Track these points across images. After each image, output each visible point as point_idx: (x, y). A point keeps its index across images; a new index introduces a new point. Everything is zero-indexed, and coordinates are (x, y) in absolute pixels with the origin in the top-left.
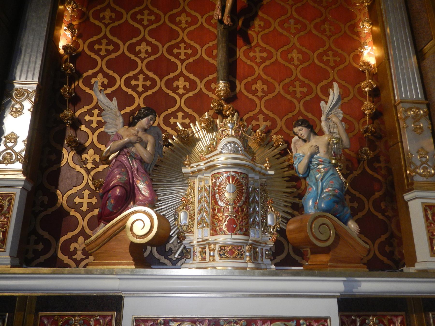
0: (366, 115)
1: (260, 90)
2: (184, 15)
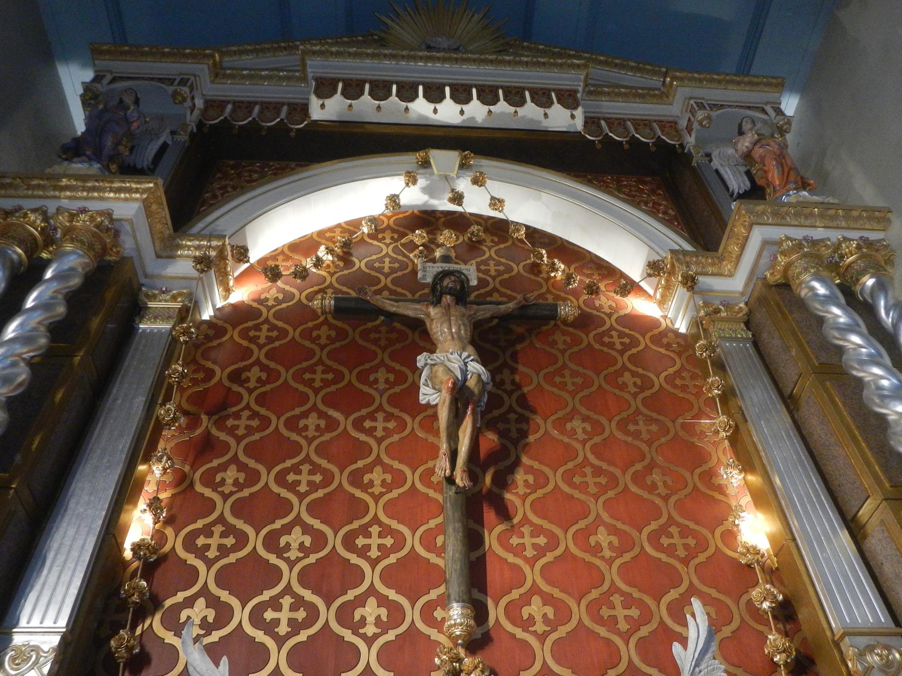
0: (776, 665)
1: (538, 618)
2: (378, 469)
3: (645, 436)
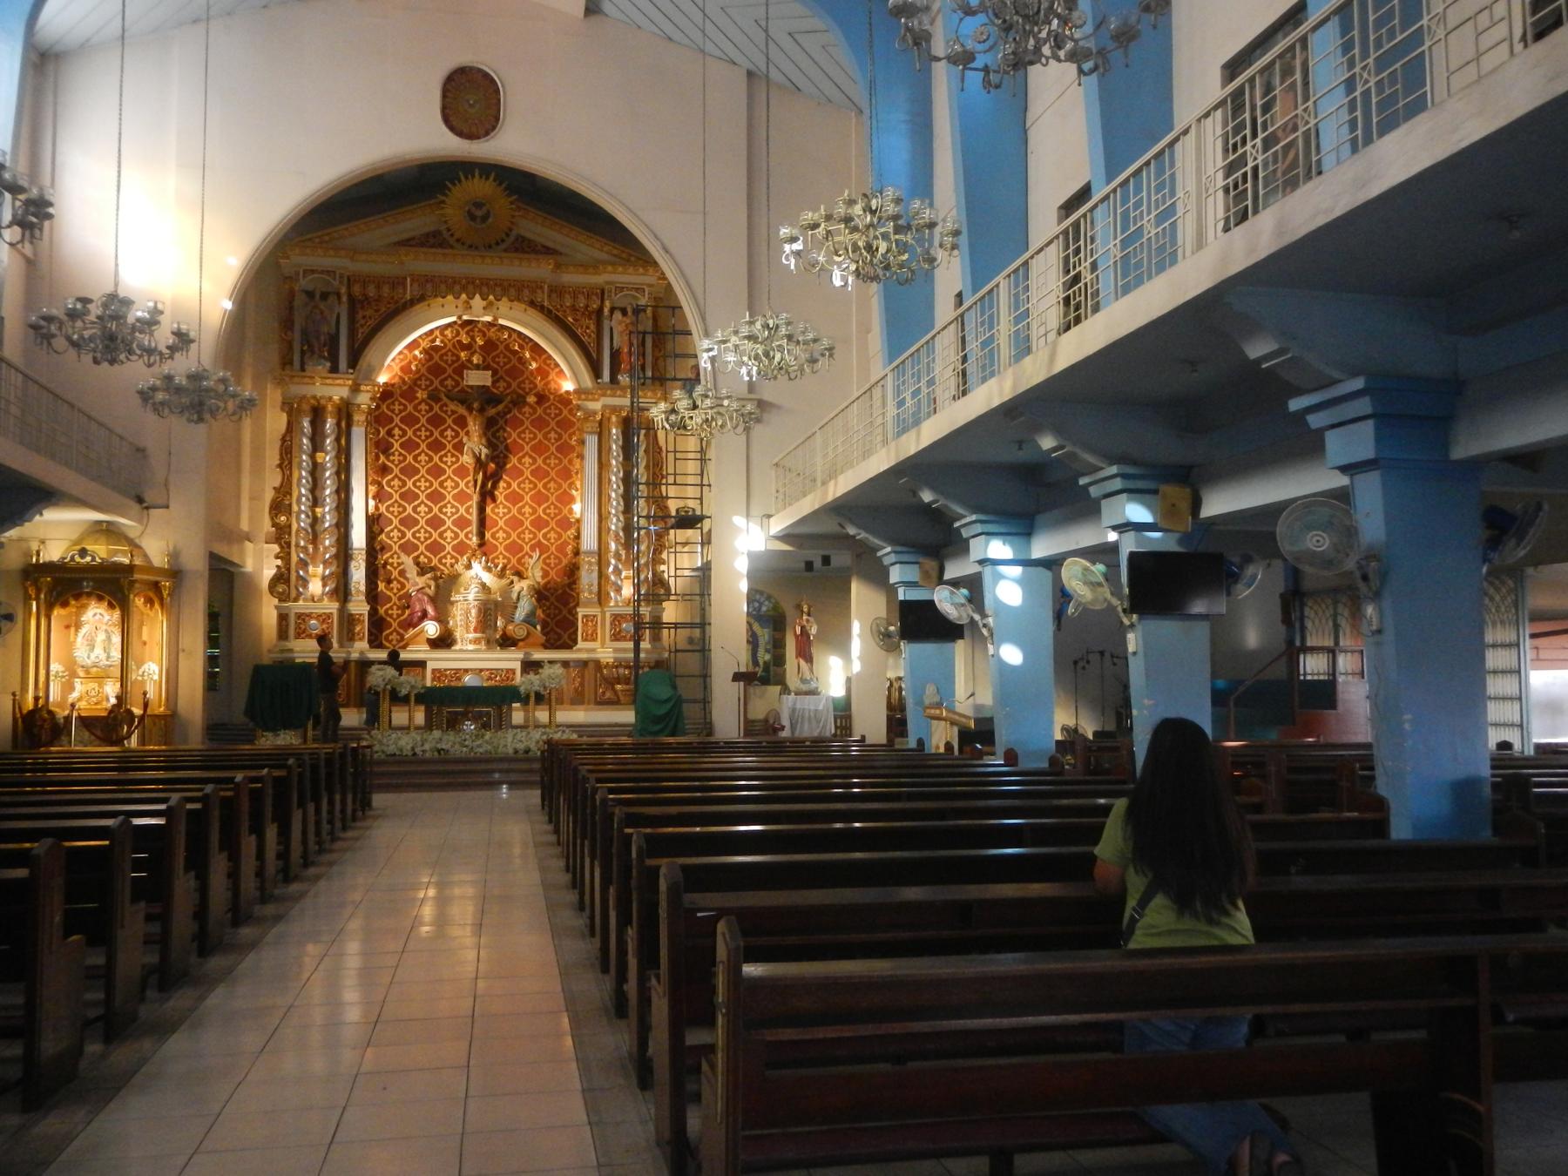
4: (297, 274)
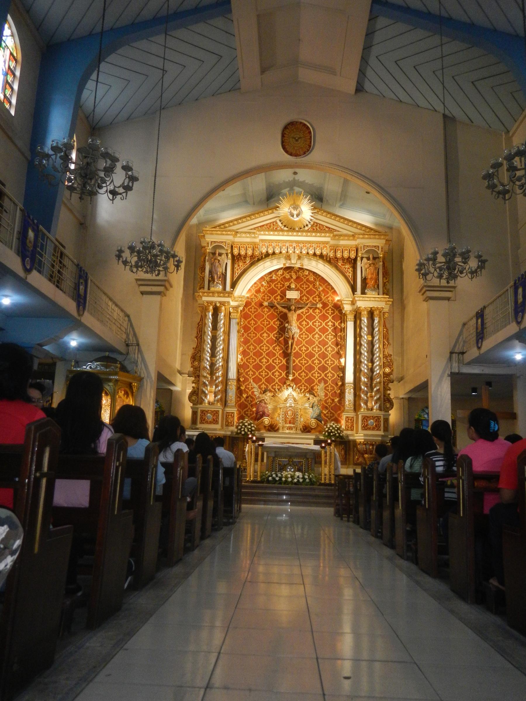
3: (330, 339)
4: (208, 244)
